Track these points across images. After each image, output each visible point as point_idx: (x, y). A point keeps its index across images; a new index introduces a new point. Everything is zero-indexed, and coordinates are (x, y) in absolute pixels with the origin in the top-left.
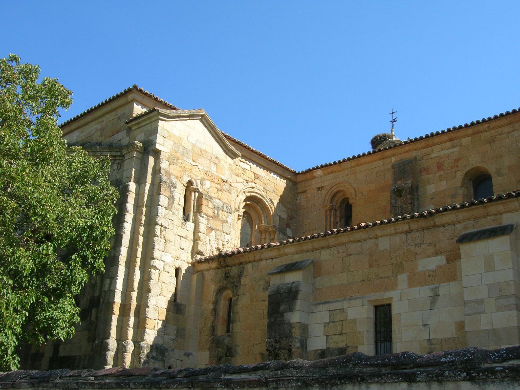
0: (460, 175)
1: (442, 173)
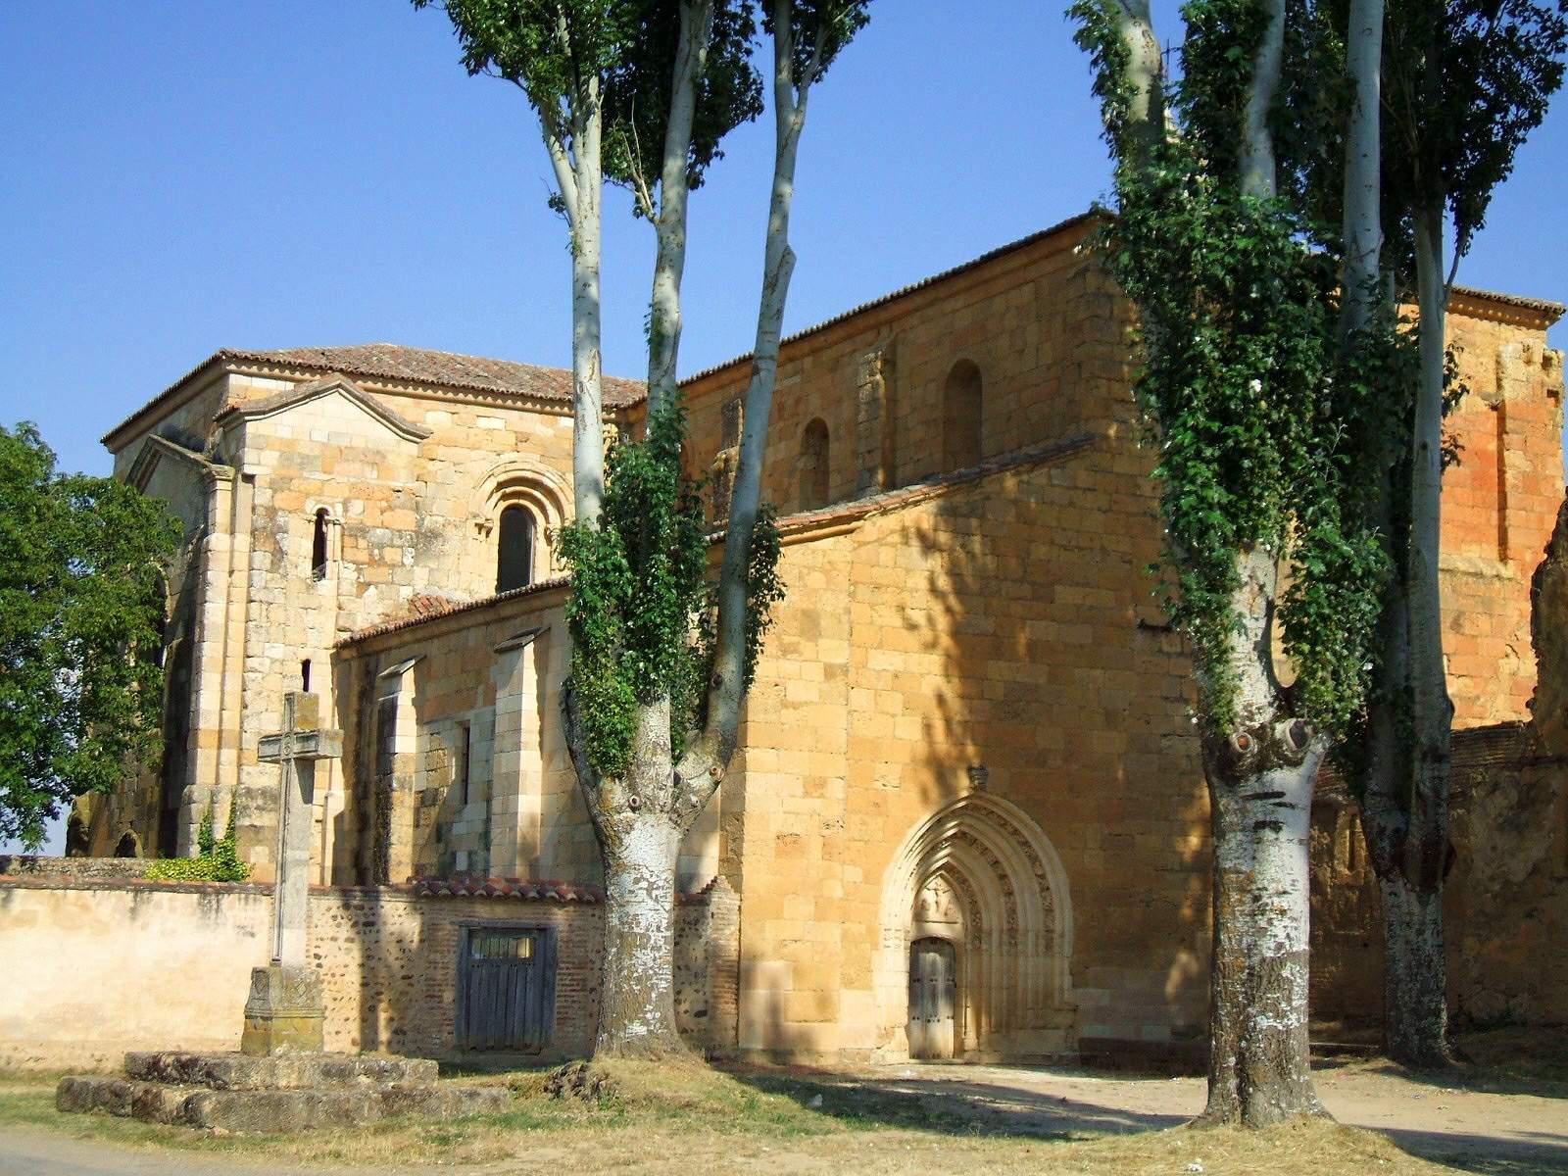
0: (800, 430)
1: (781, 424)
